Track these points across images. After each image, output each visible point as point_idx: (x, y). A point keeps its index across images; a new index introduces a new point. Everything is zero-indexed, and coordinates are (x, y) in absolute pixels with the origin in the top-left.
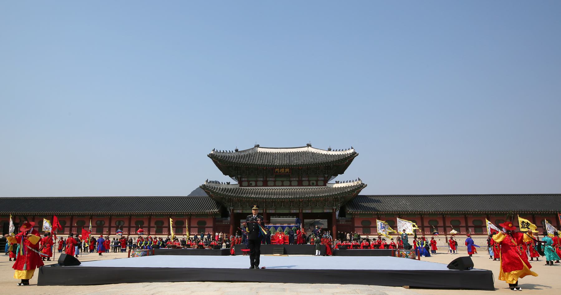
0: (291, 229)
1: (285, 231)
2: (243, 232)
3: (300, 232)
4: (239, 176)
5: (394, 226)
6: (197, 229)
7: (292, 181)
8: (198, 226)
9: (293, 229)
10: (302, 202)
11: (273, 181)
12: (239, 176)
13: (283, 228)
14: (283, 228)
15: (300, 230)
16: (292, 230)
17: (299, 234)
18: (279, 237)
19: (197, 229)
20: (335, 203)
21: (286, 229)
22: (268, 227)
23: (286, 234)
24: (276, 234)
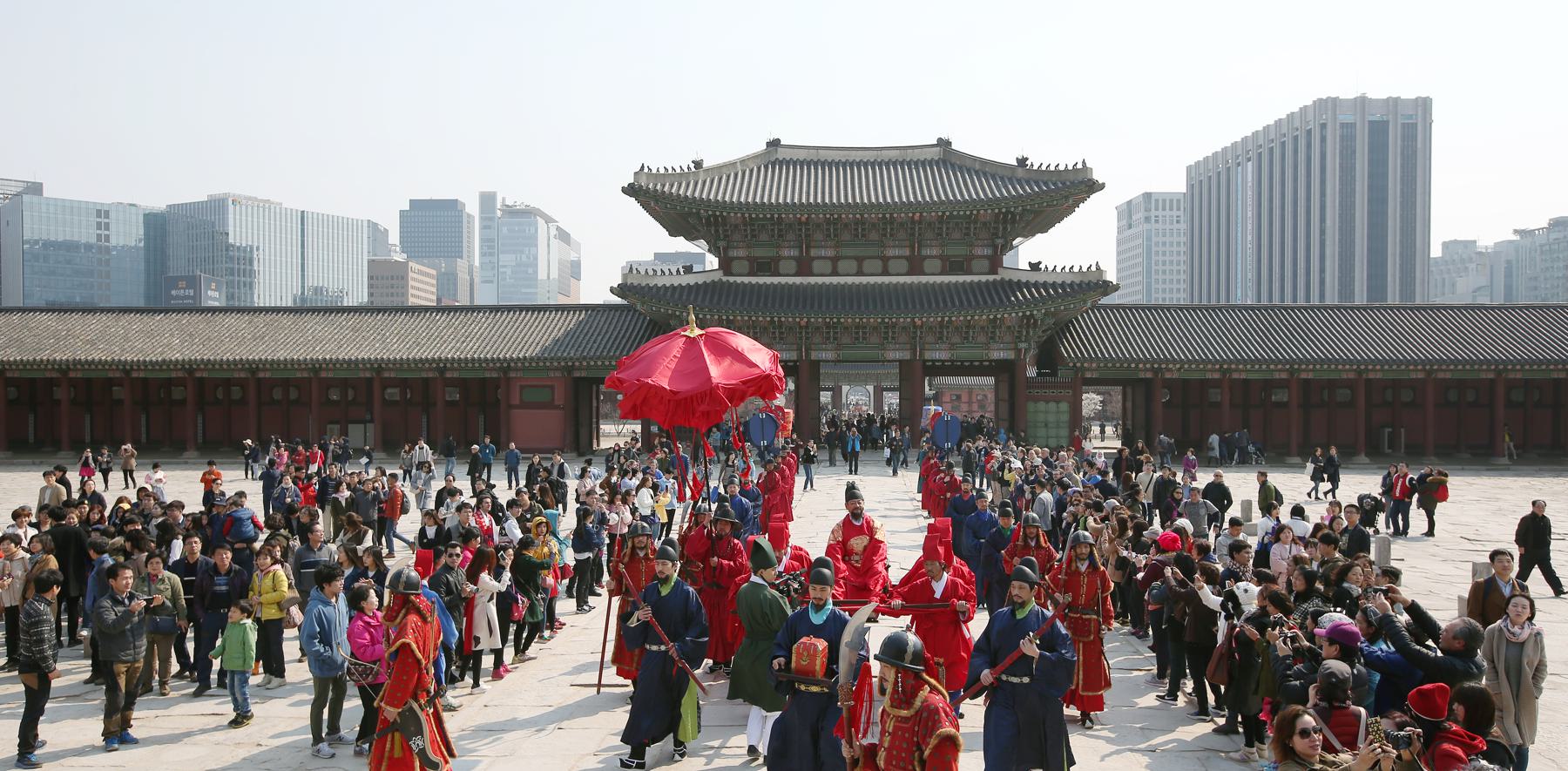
4: (722, 244)
7: (889, 258)
10: (922, 327)
11: (829, 258)
12: (722, 244)
20: (1024, 333)
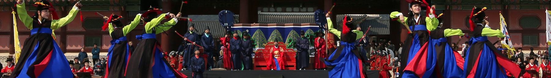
0: (304, 34)
1: (287, 40)
2: (187, 42)
3: (322, 43)
5: (539, 29)
6: (82, 37)
8: (84, 30)
9: (306, 36)
13: (284, 33)
14: (284, 33)
15: (322, 37)
16: (305, 38)
17: (320, 46)
18: (273, 54)
19: (82, 37)
21: (291, 35)
22: (247, 31)
23: (290, 46)
24: (266, 47)
